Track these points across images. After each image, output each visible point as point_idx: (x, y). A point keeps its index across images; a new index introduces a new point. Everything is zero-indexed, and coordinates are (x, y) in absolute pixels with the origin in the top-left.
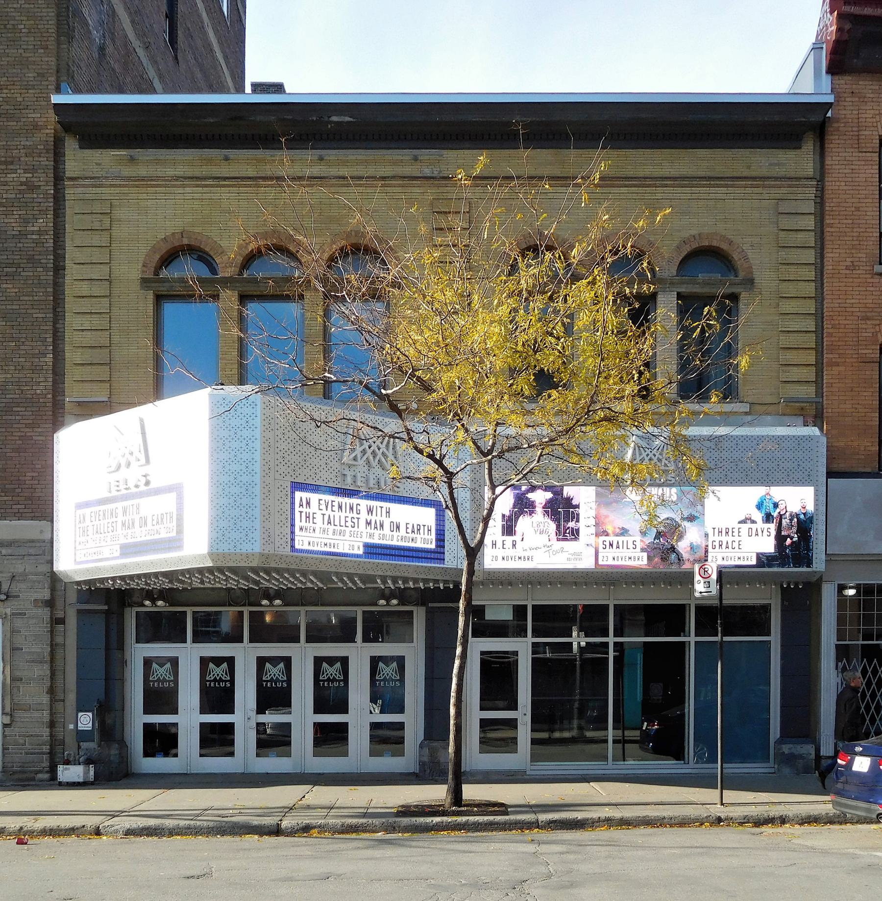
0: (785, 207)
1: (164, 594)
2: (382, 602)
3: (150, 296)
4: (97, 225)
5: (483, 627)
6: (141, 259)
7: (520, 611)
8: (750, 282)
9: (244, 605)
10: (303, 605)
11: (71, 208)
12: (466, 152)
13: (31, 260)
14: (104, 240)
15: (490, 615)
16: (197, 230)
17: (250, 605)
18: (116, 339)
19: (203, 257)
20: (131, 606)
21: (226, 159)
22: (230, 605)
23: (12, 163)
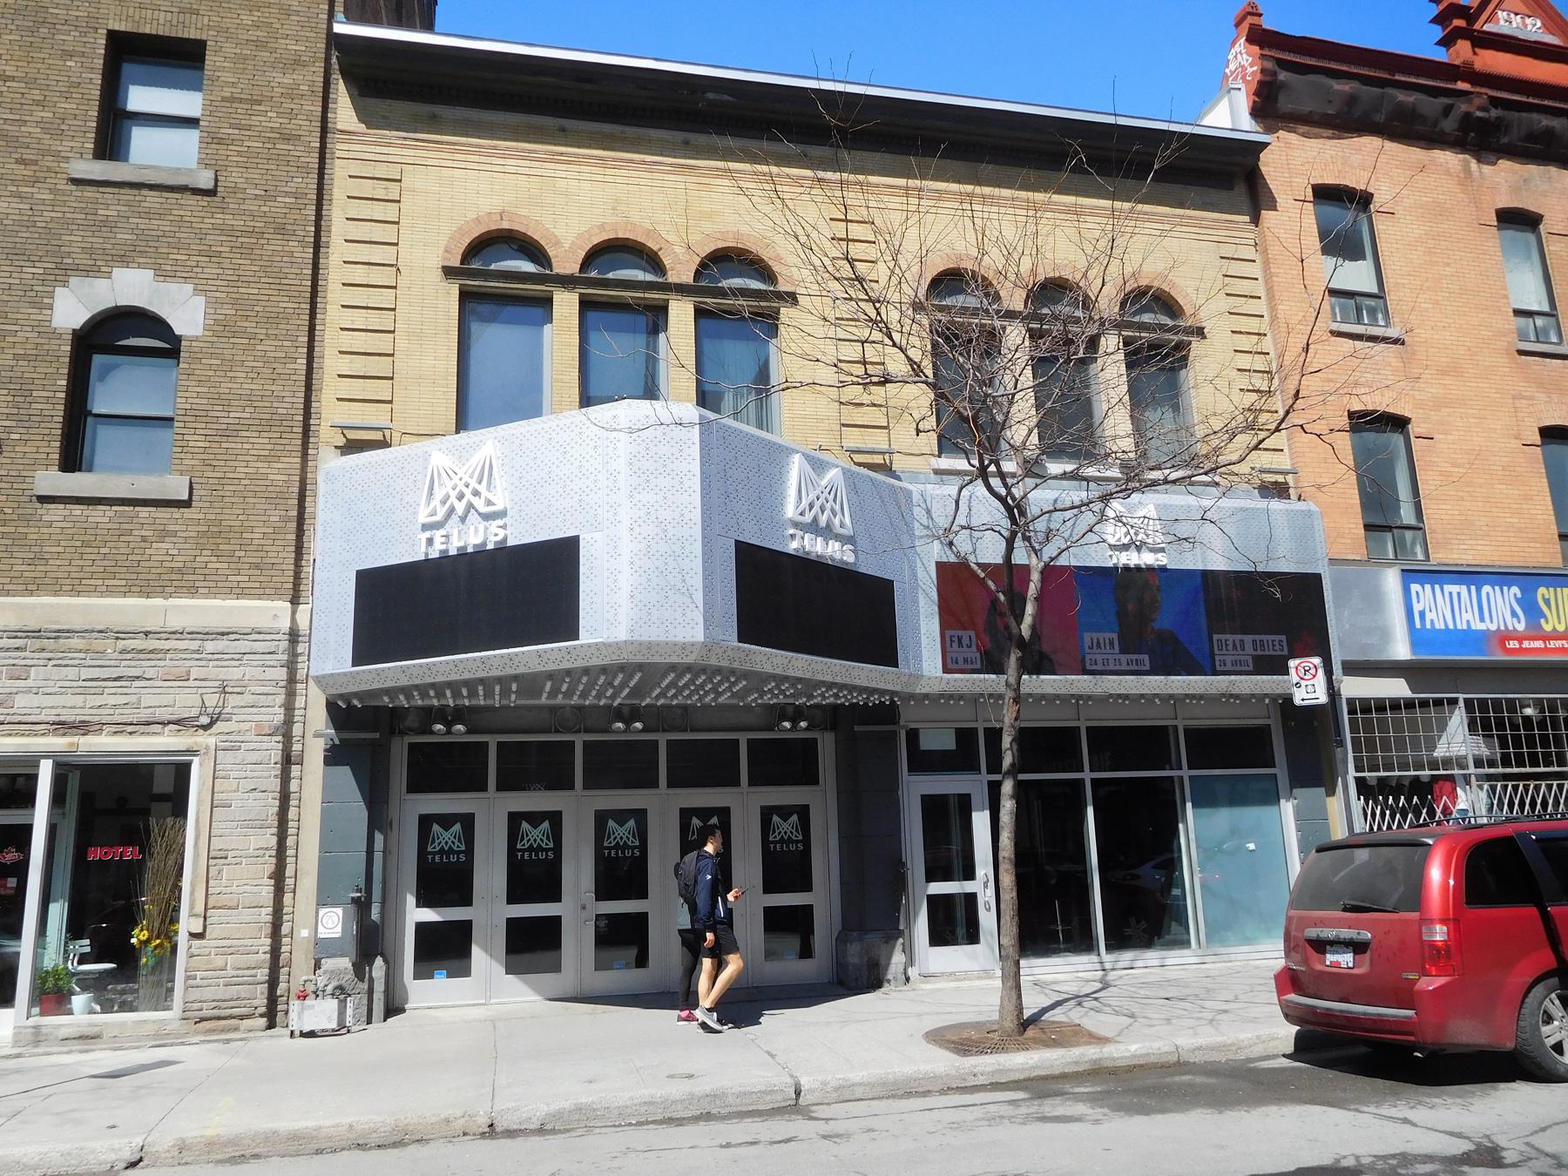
0: (1228, 251)
1: (459, 714)
2: (787, 725)
3: (455, 290)
4: (380, 194)
5: (925, 762)
6: (443, 243)
7: (965, 737)
8: (1200, 332)
9: (578, 731)
10: (664, 730)
11: (339, 171)
12: (865, 154)
13: (281, 230)
14: (390, 212)
15: (928, 742)
16: (524, 212)
17: (587, 731)
18: (401, 344)
19: (529, 248)
20: (402, 733)
21: (563, 130)
22: (557, 731)
23: (259, 103)
